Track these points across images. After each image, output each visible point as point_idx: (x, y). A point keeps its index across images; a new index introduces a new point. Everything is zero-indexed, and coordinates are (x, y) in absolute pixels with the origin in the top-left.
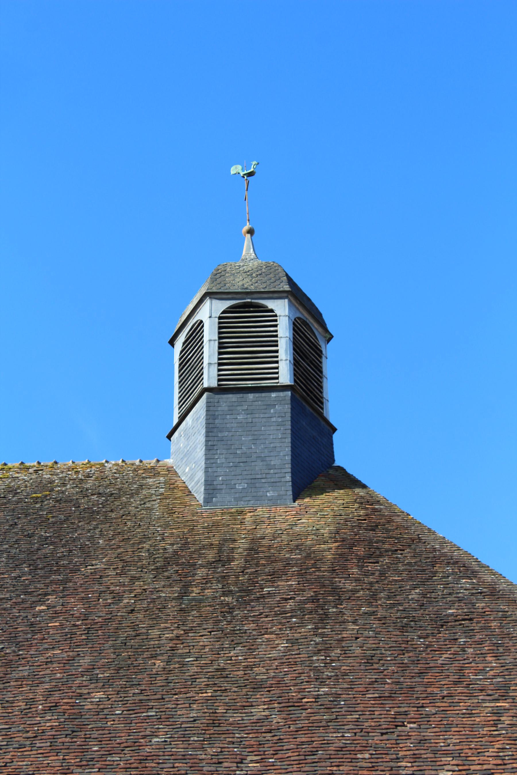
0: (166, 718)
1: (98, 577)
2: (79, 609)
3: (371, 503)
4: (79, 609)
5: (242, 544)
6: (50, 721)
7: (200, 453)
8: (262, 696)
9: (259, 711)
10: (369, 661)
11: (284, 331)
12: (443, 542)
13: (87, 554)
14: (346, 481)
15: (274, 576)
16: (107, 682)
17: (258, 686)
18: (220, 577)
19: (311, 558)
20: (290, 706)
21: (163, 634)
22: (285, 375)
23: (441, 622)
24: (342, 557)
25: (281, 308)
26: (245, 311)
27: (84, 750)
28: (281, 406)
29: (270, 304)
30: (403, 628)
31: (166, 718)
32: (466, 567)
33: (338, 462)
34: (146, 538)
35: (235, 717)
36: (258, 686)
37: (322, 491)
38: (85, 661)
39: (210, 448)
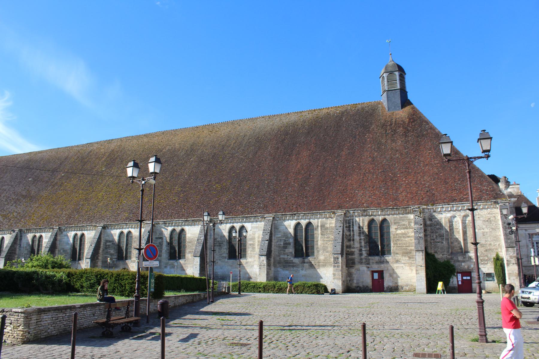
0: (385, 158)
1: (373, 129)
2: (371, 136)
3: (414, 108)
4: (371, 136)
5: (394, 120)
6: (370, 159)
7: (386, 101)
8: (397, 153)
9: (397, 155)
10: (412, 144)
11: (398, 78)
12: (424, 117)
13: (371, 124)
14: (410, 103)
15: (399, 127)
16: (377, 151)
17: (397, 151)
18: (391, 127)
19: (404, 122)
20: (401, 154)
21: (383, 141)
22: (399, 87)
23: (423, 135)
24: (409, 122)
25: (397, 74)
26: (391, 73)
27: (375, 164)
28: (398, 92)
29: (395, 73)
30: (418, 137)
31: (385, 158)
32: (427, 122)
33: (409, 98)
34: (380, 120)
35: (394, 157)
36: (397, 151)
37: (406, 106)
38: (373, 147)
39: (388, 101)
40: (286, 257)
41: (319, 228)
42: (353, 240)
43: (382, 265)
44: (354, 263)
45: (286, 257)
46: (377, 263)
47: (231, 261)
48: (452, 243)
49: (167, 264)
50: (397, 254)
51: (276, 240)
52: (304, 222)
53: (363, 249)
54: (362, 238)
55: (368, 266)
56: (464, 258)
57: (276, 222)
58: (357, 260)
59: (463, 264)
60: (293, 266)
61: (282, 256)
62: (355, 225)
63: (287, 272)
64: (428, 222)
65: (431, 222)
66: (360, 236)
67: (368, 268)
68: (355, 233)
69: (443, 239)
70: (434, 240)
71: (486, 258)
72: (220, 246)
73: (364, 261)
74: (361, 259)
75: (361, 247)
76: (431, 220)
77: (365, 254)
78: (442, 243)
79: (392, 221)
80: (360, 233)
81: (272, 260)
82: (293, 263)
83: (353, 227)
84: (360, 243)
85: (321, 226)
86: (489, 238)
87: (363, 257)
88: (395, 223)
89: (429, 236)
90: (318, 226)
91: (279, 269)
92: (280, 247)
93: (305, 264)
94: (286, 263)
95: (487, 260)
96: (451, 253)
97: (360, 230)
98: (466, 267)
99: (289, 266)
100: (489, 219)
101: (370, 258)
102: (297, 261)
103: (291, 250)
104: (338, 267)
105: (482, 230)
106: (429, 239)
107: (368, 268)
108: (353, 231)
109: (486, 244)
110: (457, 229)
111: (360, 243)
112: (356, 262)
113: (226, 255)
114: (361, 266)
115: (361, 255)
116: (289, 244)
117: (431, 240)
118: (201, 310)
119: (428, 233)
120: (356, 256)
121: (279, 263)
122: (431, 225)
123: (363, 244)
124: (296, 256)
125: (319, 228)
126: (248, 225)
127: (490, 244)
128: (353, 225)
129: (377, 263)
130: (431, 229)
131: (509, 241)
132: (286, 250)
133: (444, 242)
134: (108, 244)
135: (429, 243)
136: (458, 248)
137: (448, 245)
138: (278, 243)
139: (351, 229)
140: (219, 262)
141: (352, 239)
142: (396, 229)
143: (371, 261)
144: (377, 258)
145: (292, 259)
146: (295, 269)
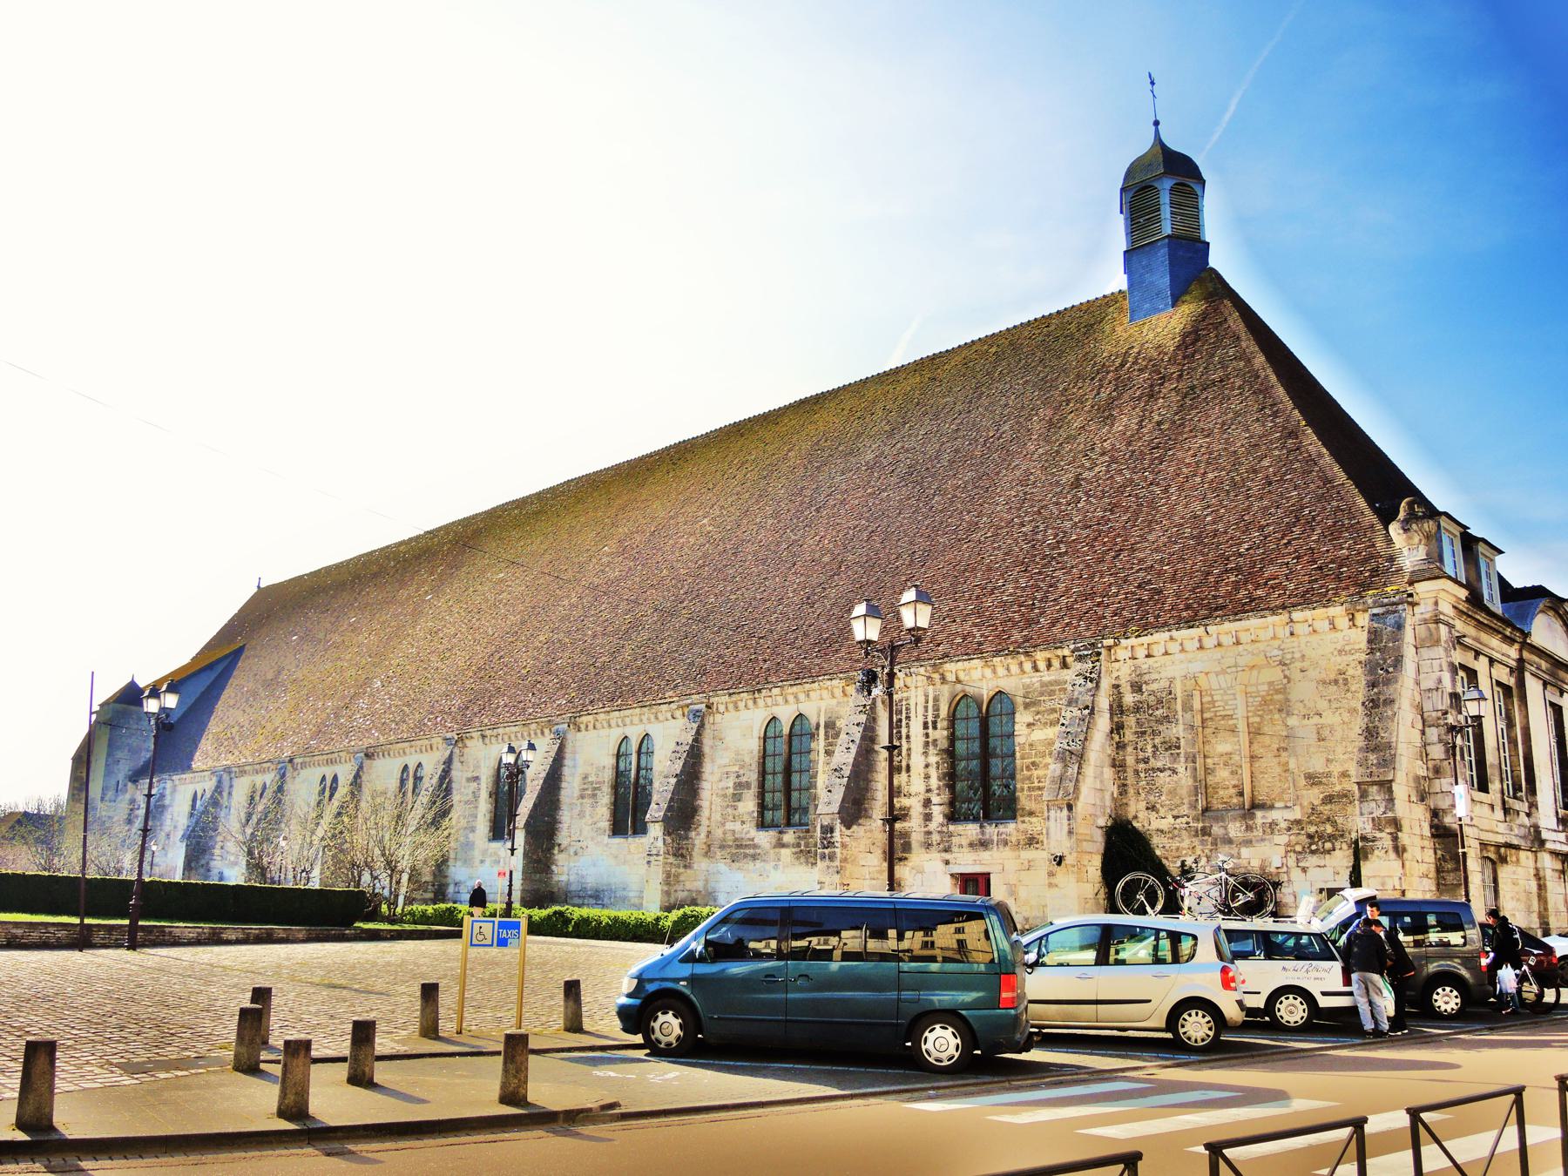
40: (737, 826)
41: (822, 731)
42: (908, 769)
43: (985, 855)
44: (907, 847)
45: (737, 826)
46: (971, 845)
47: (618, 840)
48: (1208, 771)
49: (484, 852)
50: (1031, 814)
51: (716, 778)
52: (786, 715)
53: (935, 799)
54: (933, 759)
55: (947, 856)
56: (1249, 828)
57: (718, 717)
58: (916, 838)
59: (1245, 852)
60: (754, 857)
61: (729, 826)
62: (912, 715)
63: (739, 876)
64: (1129, 699)
65: (1138, 697)
66: (925, 754)
67: (947, 863)
68: (913, 746)
69: (1175, 758)
70: (1146, 761)
71: (1329, 829)
72: (594, 796)
73: (936, 838)
74: (929, 833)
75: (929, 791)
76: (1137, 687)
77: (938, 813)
78: (1174, 772)
79: (1019, 700)
80: (927, 744)
81: (698, 838)
82: (755, 846)
83: (908, 726)
84: (927, 777)
85: (826, 726)
86: (1340, 750)
87: (933, 826)
88: (1027, 706)
89: (1130, 749)
90: (818, 727)
91: (722, 866)
92: (725, 796)
93: (783, 851)
94: (739, 847)
95: (1331, 838)
96: (1206, 810)
97: (927, 735)
98: (1256, 864)
99: (746, 856)
100: (1342, 673)
101: (951, 828)
102: (765, 838)
103: (749, 805)
104: (832, 857)
105: (1316, 719)
106: (1130, 760)
107: (947, 863)
108: (908, 737)
109: (1328, 775)
110: (1231, 717)
111: (927, 777)
112: (914, 845)
113: (605, 824)
114: (928, 856)
115: (928, 817)
116: (748, 785)
117: (1138, 761)
118: (981, 994)
119: (1129, 735)
120: (914, 825)
121: (722, 847)
122: (1137, 709)
123: (934, 782)
124: (762, 825)
125: (822, 731)
126: (655, 730)
127: (1345, 775)
128: (908, 718)
129: (971, 845)
130: (1138, 722)
131: (1373, 758)
132: (740, 805)
133: (1181, 768)
134: (378, 800)
135: (1130, 773)
136: (1233, 791)
137: (1195, 778)
138: (721, 785)
139: (904, 731)
140: (590, 844)
141: (904, 764)
142: (1029, 725)
143: (955, 840)
144: (971, 830)
145: (753, 832)
146: (758, 864)
